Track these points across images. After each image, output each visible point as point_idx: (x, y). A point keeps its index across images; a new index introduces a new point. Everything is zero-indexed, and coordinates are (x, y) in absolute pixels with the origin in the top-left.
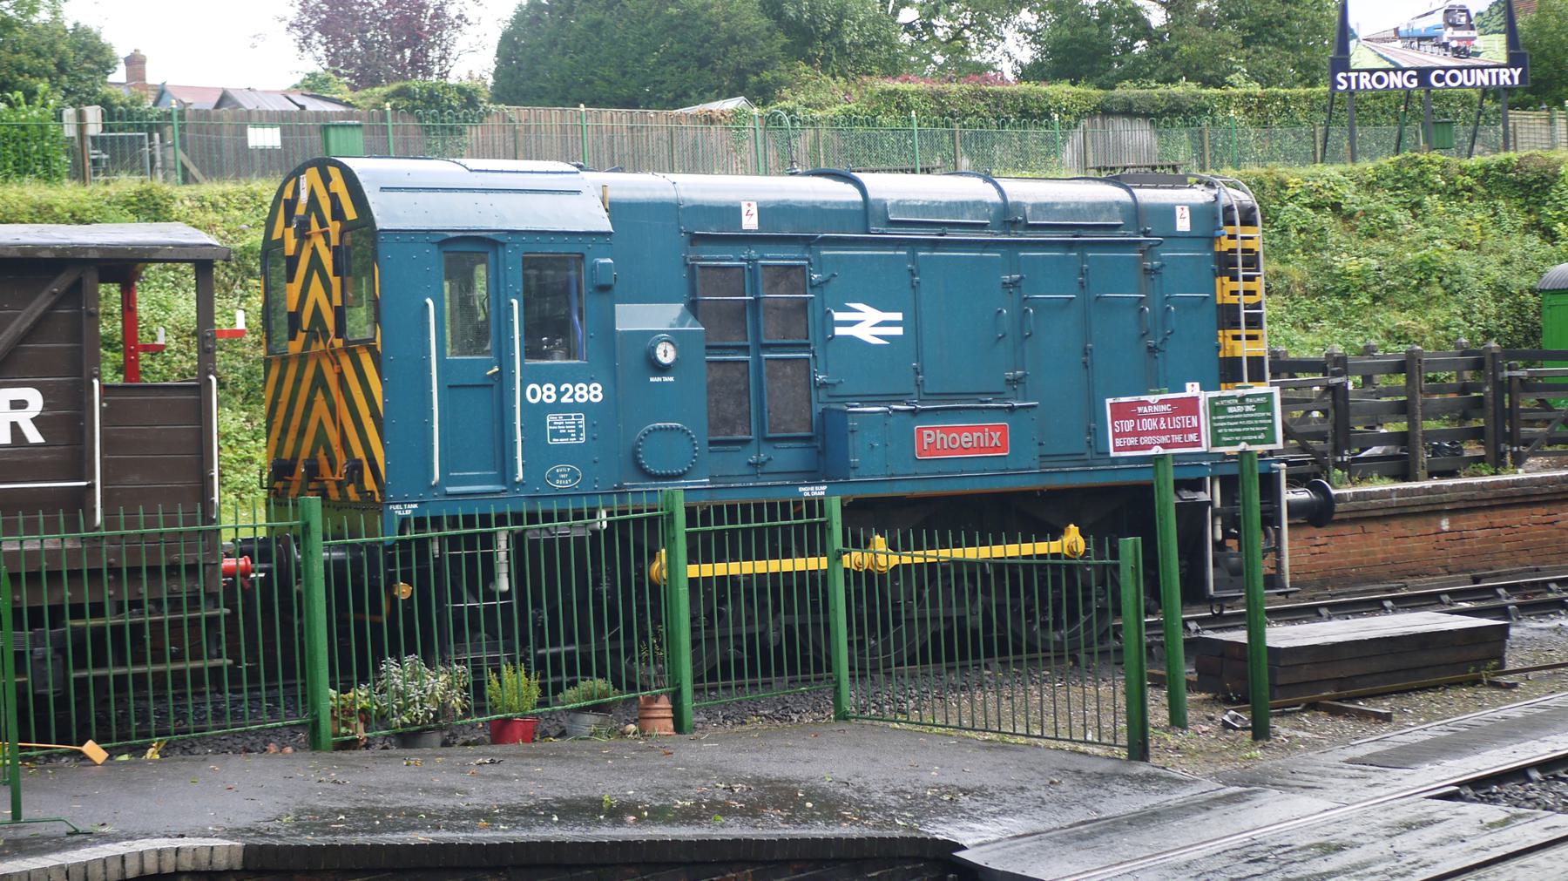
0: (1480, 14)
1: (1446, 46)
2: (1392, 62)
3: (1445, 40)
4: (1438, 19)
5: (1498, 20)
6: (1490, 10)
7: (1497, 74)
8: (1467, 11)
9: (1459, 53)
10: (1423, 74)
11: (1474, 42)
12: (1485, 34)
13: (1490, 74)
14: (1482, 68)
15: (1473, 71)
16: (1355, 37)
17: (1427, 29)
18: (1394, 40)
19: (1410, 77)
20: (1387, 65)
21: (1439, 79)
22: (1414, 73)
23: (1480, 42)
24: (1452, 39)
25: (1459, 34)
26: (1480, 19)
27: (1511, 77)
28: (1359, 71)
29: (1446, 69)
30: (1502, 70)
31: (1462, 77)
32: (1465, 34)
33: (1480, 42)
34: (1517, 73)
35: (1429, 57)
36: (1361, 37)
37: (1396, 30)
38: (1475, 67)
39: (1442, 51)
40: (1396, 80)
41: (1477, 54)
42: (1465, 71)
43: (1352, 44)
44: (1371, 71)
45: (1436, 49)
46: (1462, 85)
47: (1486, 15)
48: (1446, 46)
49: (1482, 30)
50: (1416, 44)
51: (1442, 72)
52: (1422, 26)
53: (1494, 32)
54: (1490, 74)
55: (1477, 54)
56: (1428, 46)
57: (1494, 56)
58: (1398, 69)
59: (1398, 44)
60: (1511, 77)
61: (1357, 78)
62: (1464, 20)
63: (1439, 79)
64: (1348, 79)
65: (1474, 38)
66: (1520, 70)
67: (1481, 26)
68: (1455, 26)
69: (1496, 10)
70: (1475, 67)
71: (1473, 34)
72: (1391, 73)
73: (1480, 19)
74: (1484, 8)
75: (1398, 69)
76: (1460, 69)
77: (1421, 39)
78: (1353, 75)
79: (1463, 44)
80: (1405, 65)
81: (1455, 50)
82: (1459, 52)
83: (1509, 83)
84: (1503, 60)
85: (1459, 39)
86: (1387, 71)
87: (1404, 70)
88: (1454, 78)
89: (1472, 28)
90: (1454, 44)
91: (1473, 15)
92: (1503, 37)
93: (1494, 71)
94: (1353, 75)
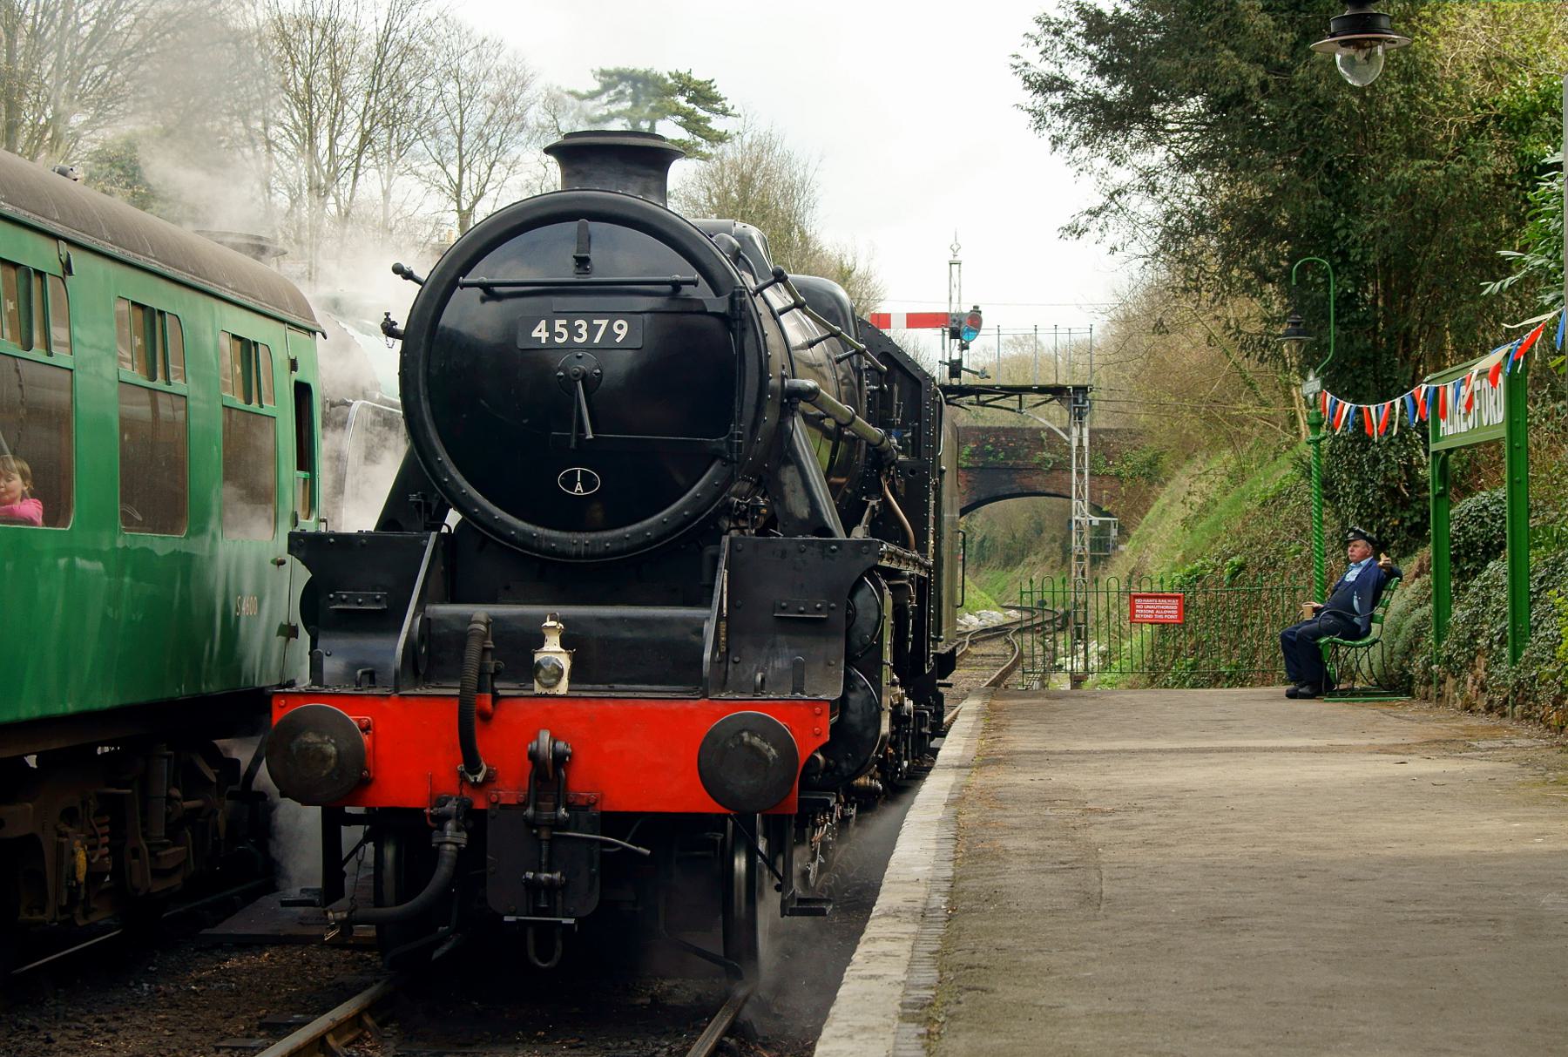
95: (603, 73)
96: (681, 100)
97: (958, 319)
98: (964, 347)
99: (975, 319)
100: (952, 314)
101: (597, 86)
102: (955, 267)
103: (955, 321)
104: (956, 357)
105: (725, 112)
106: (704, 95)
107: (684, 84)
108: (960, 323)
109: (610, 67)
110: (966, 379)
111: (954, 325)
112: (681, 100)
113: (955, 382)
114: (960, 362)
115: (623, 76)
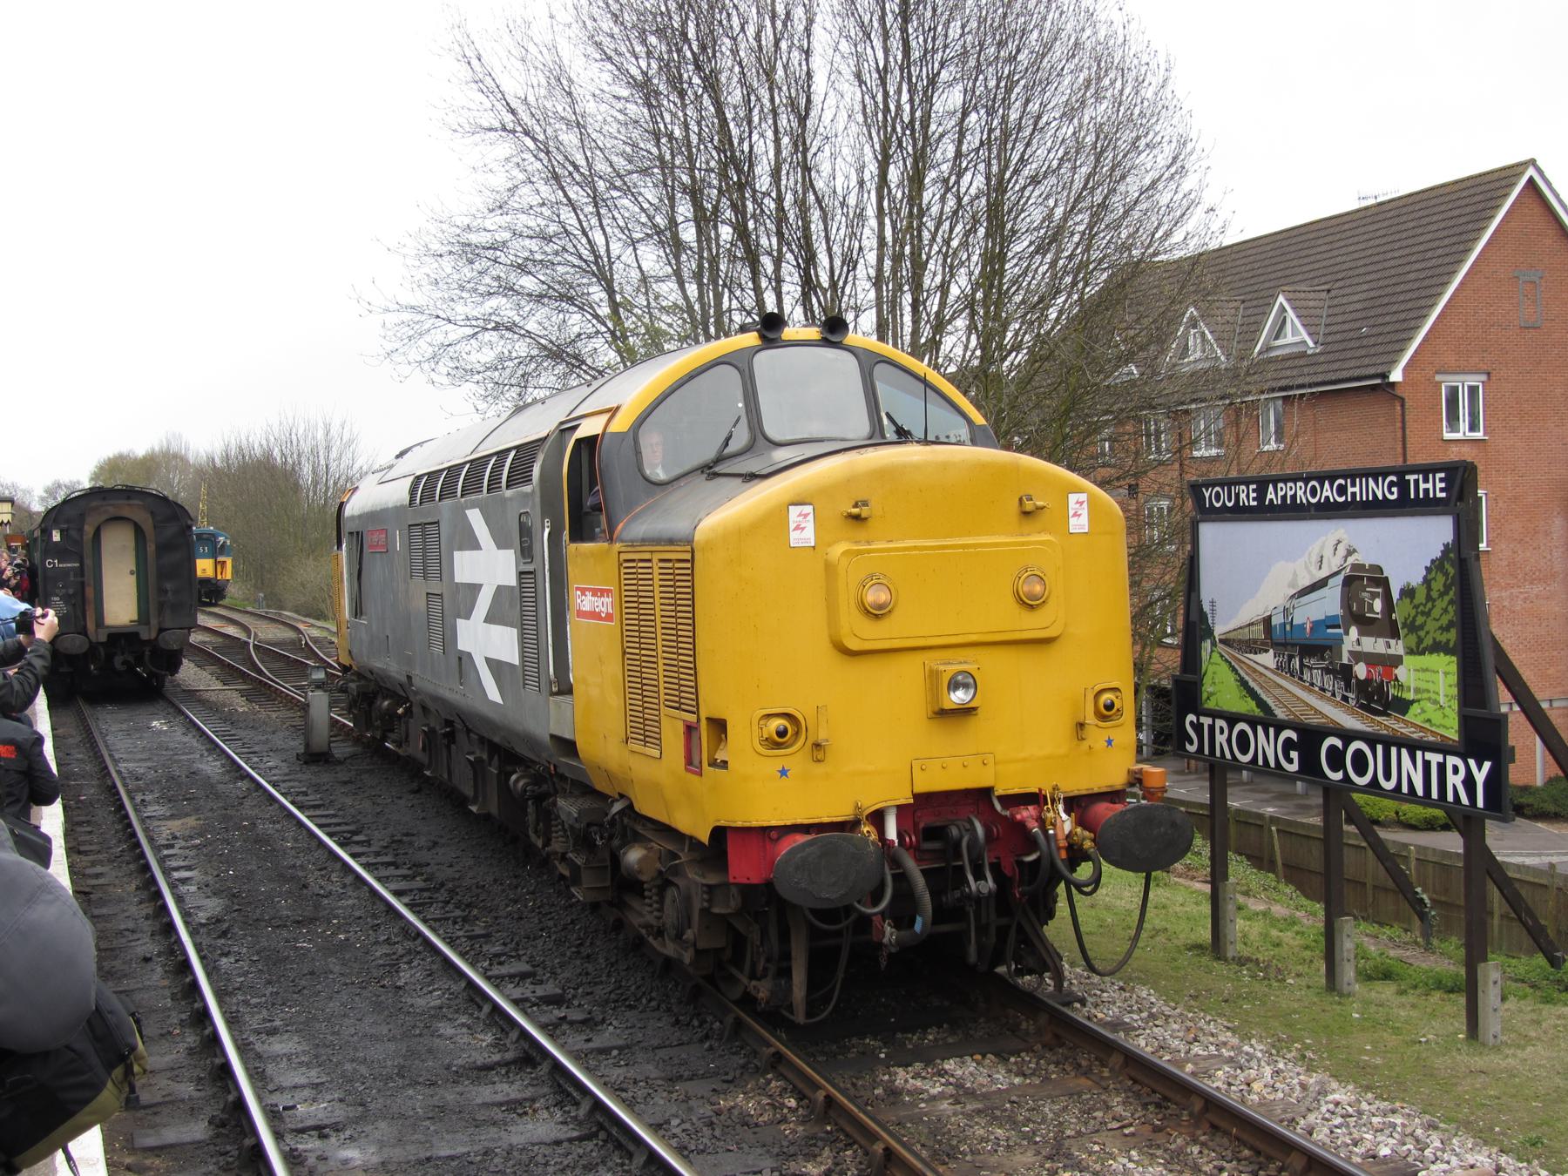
0: (1408, 592)
1: (1345, 673)
2: (1261, 704)
3: (1345, 661)
5: (1444, 611)
6: (1427, 581)
7: (1442, 767)
8: (1384, 583)
9: (1370, 698)
10: (1309, 738)
11: (1400, 672)
13: (1427, 764)
14: (1413, 747)
15: (1394, 750)
16: (1209, 633)
17: (1316, 625)
20: (1248, 706)
22: (1294, 736)
24: (1357, 656)
27: (1469, 782)
28: (1215, 714)
29: (1348, 736)
30: (1452, 760)
36: (1219, 630)
37: (1267, 621)
42: (1379, 748)
44: (1232, 719)
45: (1329, 681)
46: (1374, 781)
47: (1420, 597)
49: (1413, 639)
50: (1296, 662)
51: (1339, 743)
53: (1436, 648)
54: (1427, 764)
55: (1403, 706)
57: (1437, 717)
58: (1267, 721)
59: (1268, 659)
60: (1469, 782)
61: (1212, 728)
62: (1378, 605)
63: (1336, 759)
64: (1198, 728)
65: (1397, 661)
66: (1487, 765)
67: (1412, 627)
68: (1367, 625)
69: (1438, 585)
71: (1397, 648)
72: (1259, 728)
74: (1416, 578)
75: (1267, 721)
76: (1372, 741)
78: (1206, 721)
80: (1281, 714)
81: (1363, 686)
83: (1465, 800)
85: (1371, 659)
88: (1360, 763)
89: (1395, 634)
91: (1395, 595)
93: (1435, 758)
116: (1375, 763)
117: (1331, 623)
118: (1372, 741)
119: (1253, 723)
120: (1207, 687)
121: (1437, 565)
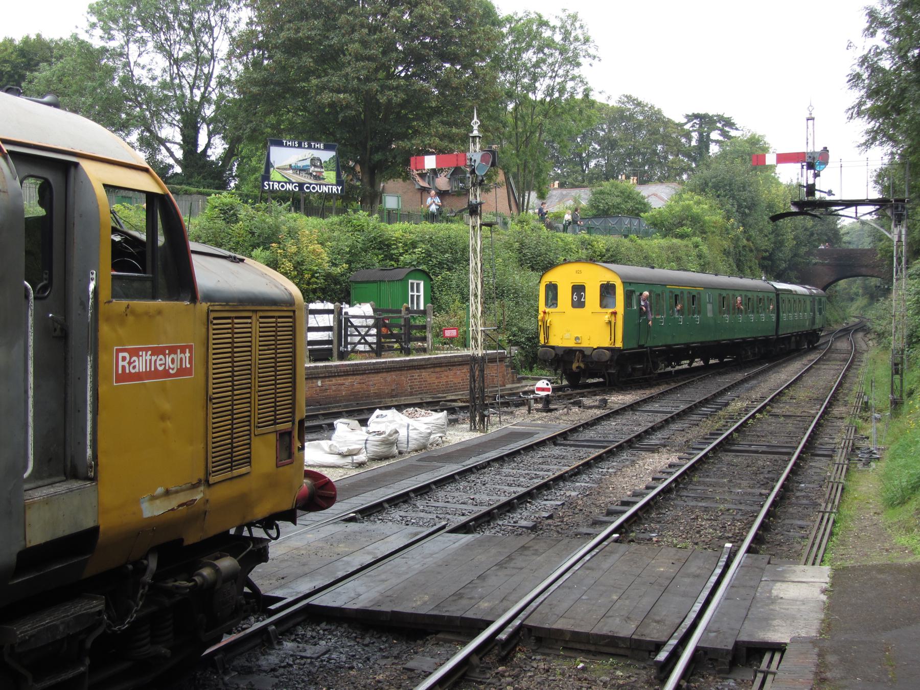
1: (311, 174)
4: (308, 162)
10: (301, 185)
12: (327, 170)
16: (273, 167)
18: (289, 169)
19: (295, 187)
21: (308, 188)
23: (325, 174)
25: (316, 169)
26: (325, 164)
27: (337, 190)
29: (311, 184)
31: (317, 188)
32: (319, 170)
33: (325, 174)
34: (340, 188)
35: (303, 178)
37: (290, 165)
38: (323, 185)
39: (309, 176)
40: (290, 187)
41: (324, 179)
43: (272, 169)
44: (279, 182)
48: (311, 174)
52: (301, 164)
53: (331, 170)
55: (324, 179)
56: (303, 174)
58: (290, 182)
59: (291, 171)
60: (337, 190)
61: (273, 185)
67: (326, 167)
68: (315, 166)
70: (323, 185)
71: (322, 170)
73: (325, 164)
74: (327, 160)
75: (290, 182)
76: (317, 185)
77: (300, 170)
78: (271, 183)
79: (318, 174)
80: (294, 181)
82: (317, 177)
84: (334, 182)
85: (316, 172)
86: (286, 183)
87: (293, 183)
88: (314, 188)
89: (322, 168)
90: (314, 174)
92: (334, 173)
93: (330, 187)
94: (271, 183)
95: (687, 116)
96: (719, 125)
97: (812, 156)
98: (816, 175)
99: (824, 156)
100: (808, 153)
101: (685, 120)
102: (810, 122)
103: (810, 157)
104: (811, 182)
105: (737, 129)
106: (729, 123)
107: (721, 118)
108: (814, 159)
109: (690, 114)
110: (818, 195)
111: (809, 161)
112: (719, 125)
113: (810, 198)
114: (814, 185)
115: (696, 116)
116: (317, 188)
117: (308, 166)
118: (317, 185)
119: (286, 183)
120: (272, 176)
121: (332, 158)
